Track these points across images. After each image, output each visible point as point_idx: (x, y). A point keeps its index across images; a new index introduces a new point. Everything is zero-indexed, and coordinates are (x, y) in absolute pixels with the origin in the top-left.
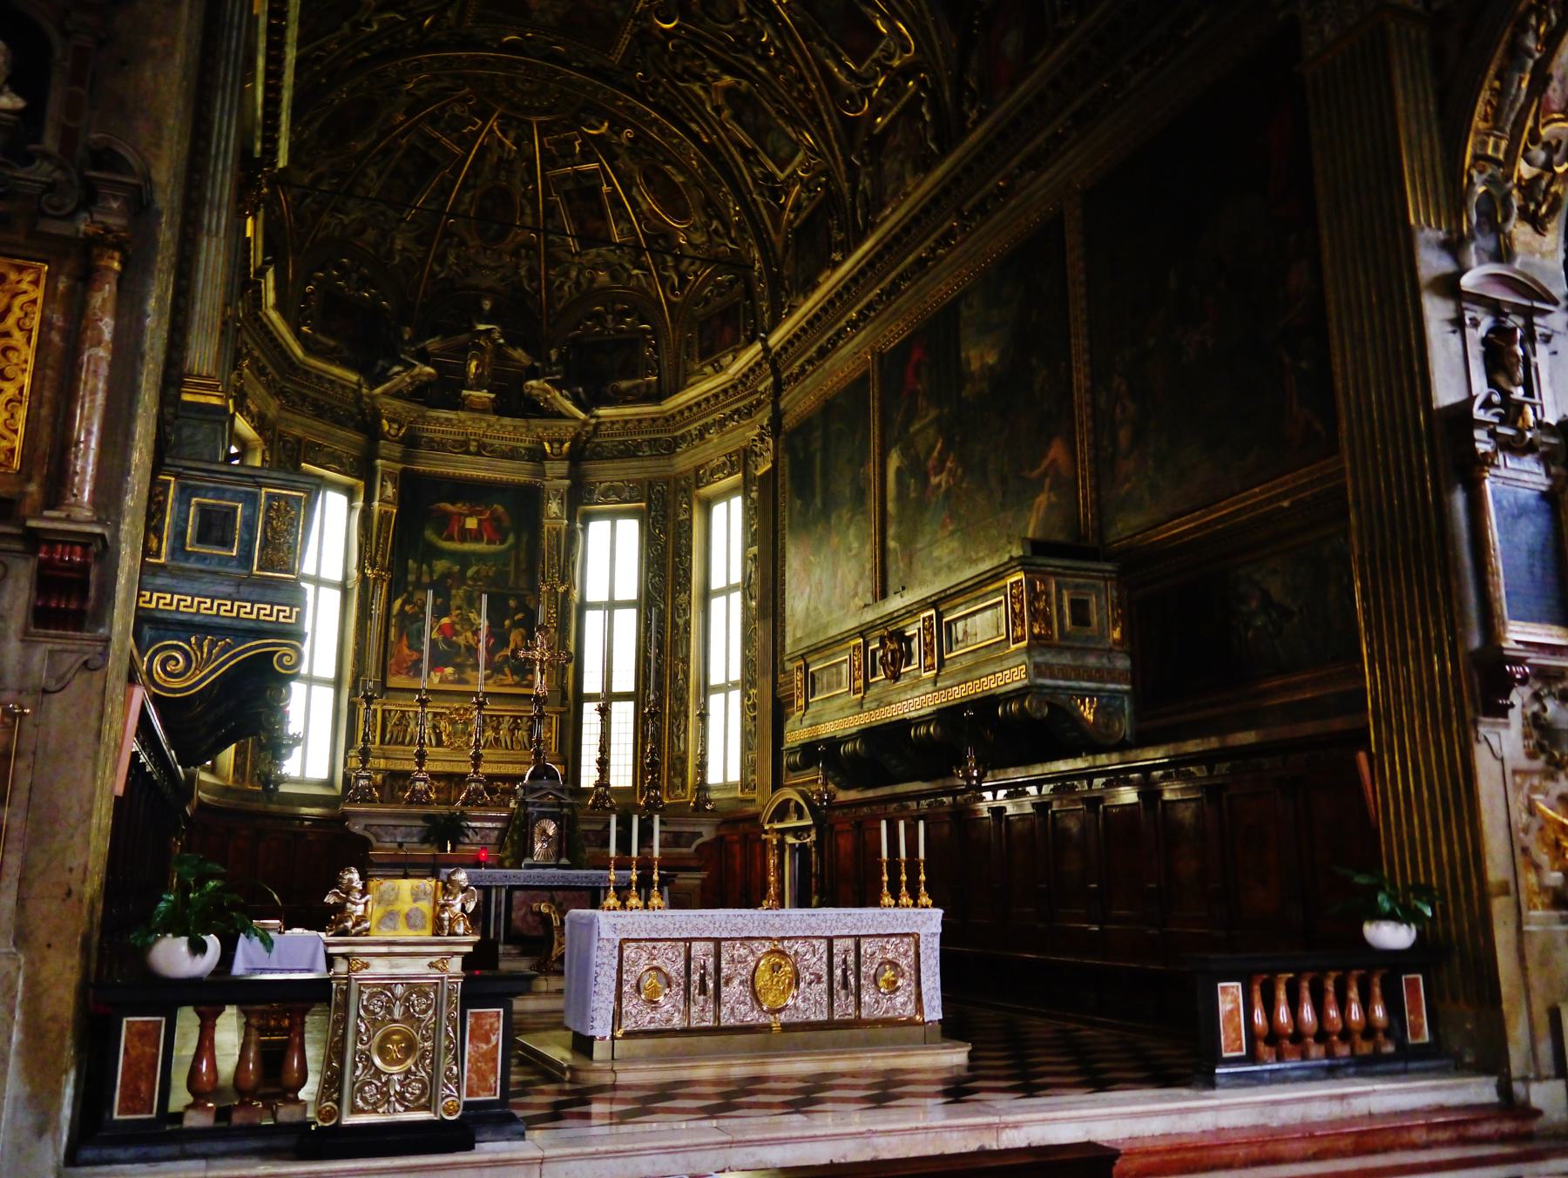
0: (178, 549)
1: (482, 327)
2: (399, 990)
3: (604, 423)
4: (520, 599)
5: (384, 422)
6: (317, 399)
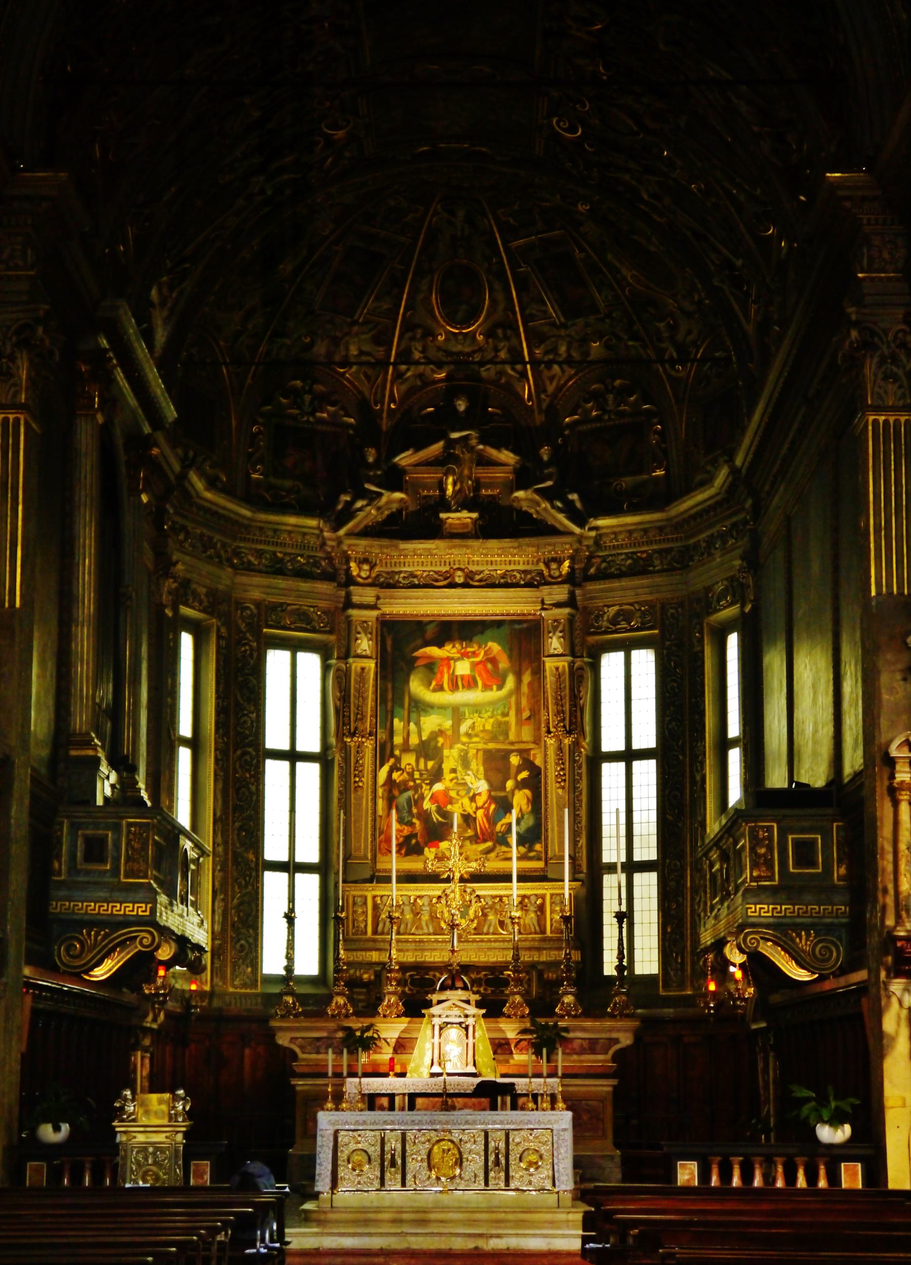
0: (73, 869)
1: (455, 435)
2: (151, 1150)
3: (606, 534)
4: (524, 753)
5: (353, 564)
6: (274, 553)
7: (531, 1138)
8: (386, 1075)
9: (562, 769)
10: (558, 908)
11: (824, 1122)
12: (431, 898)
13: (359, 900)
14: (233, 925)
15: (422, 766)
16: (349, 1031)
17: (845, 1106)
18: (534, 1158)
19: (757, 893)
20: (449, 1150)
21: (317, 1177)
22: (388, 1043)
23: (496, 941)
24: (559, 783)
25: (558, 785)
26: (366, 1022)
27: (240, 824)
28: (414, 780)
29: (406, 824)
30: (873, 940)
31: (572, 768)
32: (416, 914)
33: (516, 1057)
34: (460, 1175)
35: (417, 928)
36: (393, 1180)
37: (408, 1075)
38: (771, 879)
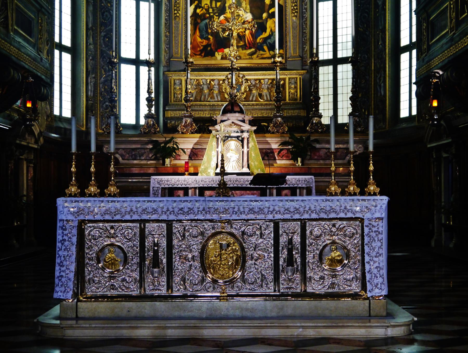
7: (334, 229)
8: (183, 174)
9: (296, 6)
10: (293, 86)
12: (219, 80)
13: (177, 82)
14: (101, 94)
15: (214, 5)
16: (156, 143)
18: (336, 254)
20: (228, 245)
21: (57, 281)
22: (184, 152)
23: (257, 105)
24: (294, 13)
25: (293, 15)
26: (168, 137)
27: (105, 34)
28: (209, 14)
29: (205, 39)
31: (301, 6)
32: (211, 89)
33: (278, 162)
34: (243, 276)
35: (211, 98)
37: (199, 174)
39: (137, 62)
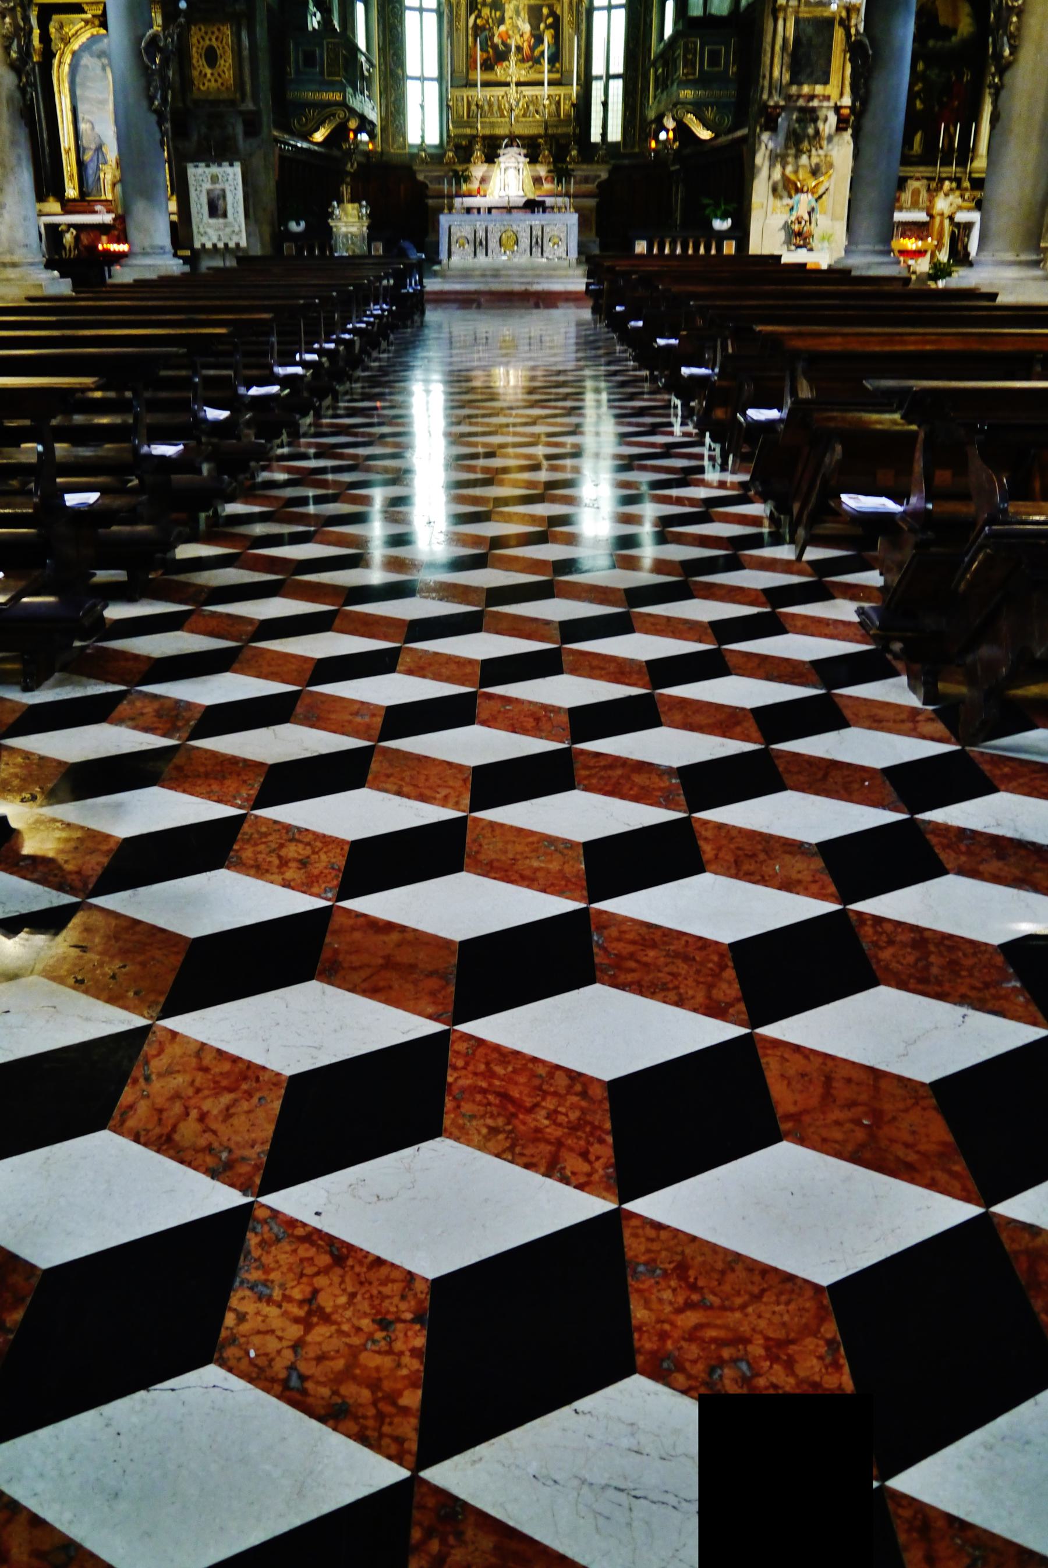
4: (551, 7)
11: (716, 217)
16: (456, 172)
17: (731, 208)
18: (556, 240)
19: (685, 84)
26: (464, 167)
30: (754, 109)
32: (490, 105)
36: (481, 252)
38: (694, 74)
39: (422, 79)
